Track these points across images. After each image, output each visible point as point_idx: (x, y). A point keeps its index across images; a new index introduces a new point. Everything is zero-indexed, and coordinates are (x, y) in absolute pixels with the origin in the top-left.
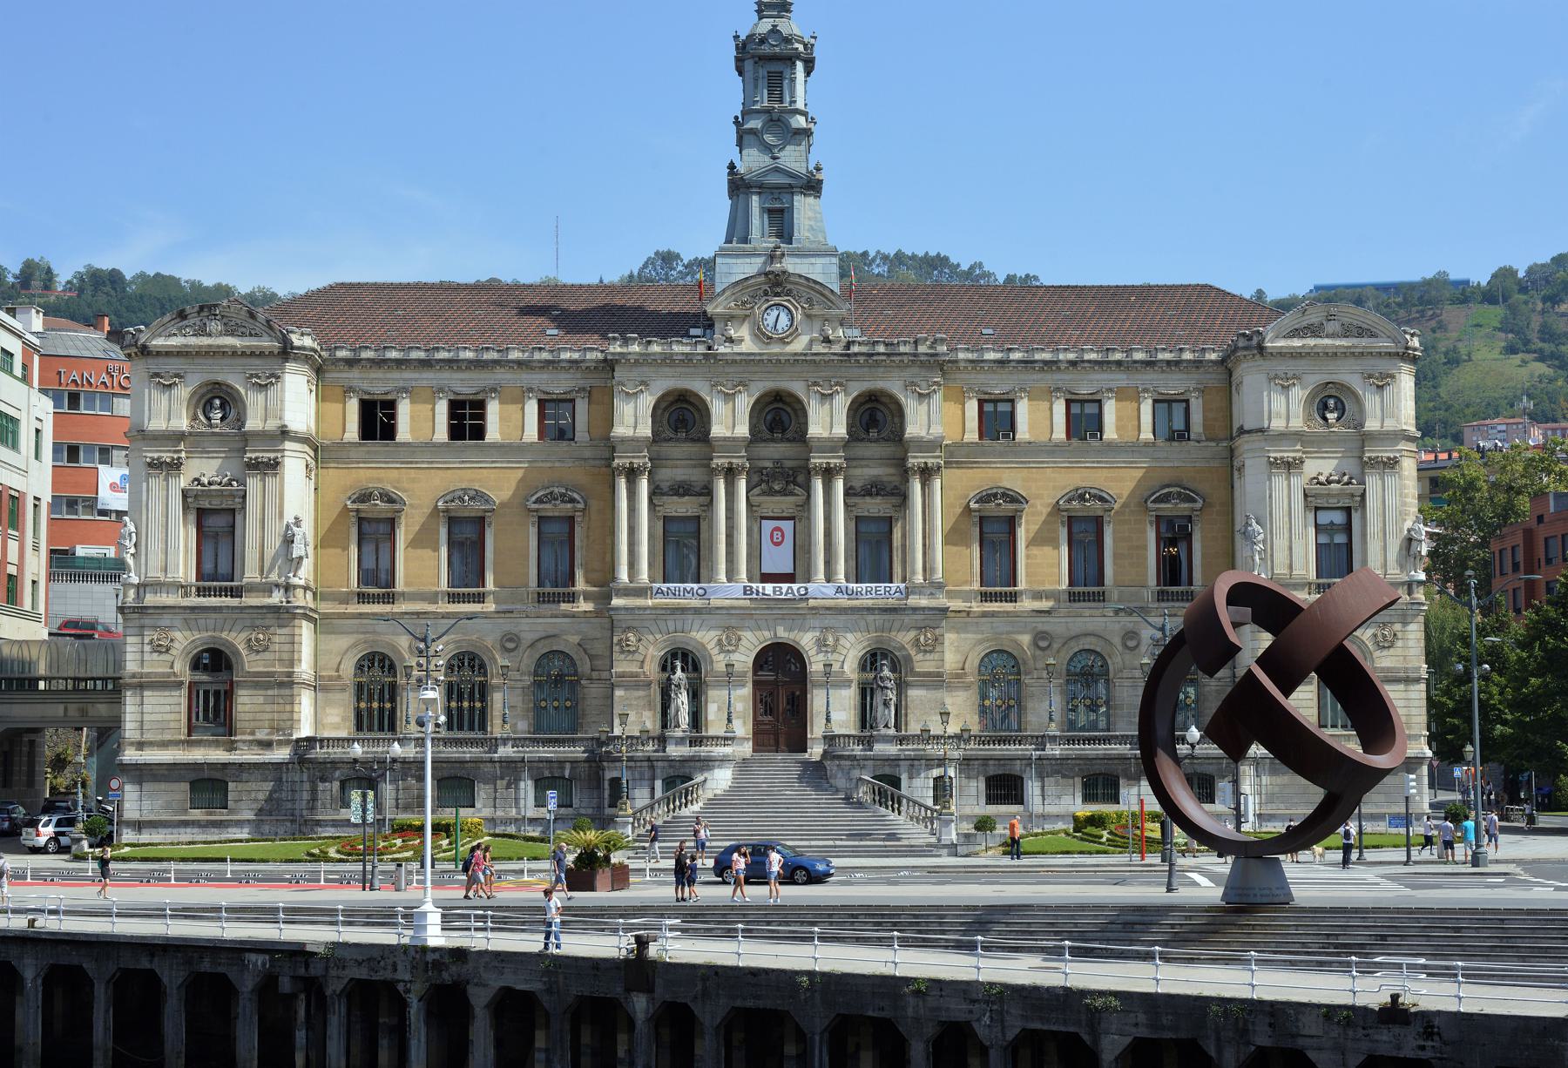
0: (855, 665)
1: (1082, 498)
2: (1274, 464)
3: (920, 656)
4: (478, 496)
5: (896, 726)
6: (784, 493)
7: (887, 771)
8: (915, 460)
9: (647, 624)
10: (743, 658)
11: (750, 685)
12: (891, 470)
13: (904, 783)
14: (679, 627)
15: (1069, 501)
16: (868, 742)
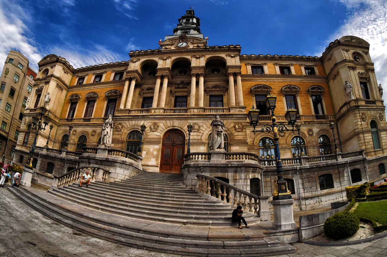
0: (207, 138)
1: (289, 88)
2: (349, 67)
3: (237, 134)
4: (95, 93)
5: (225, 148)
6: (183, 88)
7: (220, 175)
8: (230, 71)
9: (126, 122)
10: (159, 134)
11: (161, 145)
12: (221, 82)
13: (231, 183)
14: (136, 123)
15: (285, 89)
16: (209, 155)
